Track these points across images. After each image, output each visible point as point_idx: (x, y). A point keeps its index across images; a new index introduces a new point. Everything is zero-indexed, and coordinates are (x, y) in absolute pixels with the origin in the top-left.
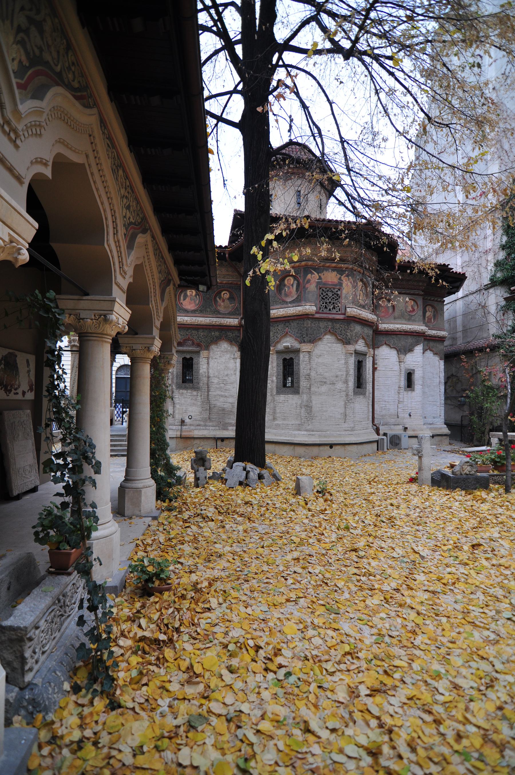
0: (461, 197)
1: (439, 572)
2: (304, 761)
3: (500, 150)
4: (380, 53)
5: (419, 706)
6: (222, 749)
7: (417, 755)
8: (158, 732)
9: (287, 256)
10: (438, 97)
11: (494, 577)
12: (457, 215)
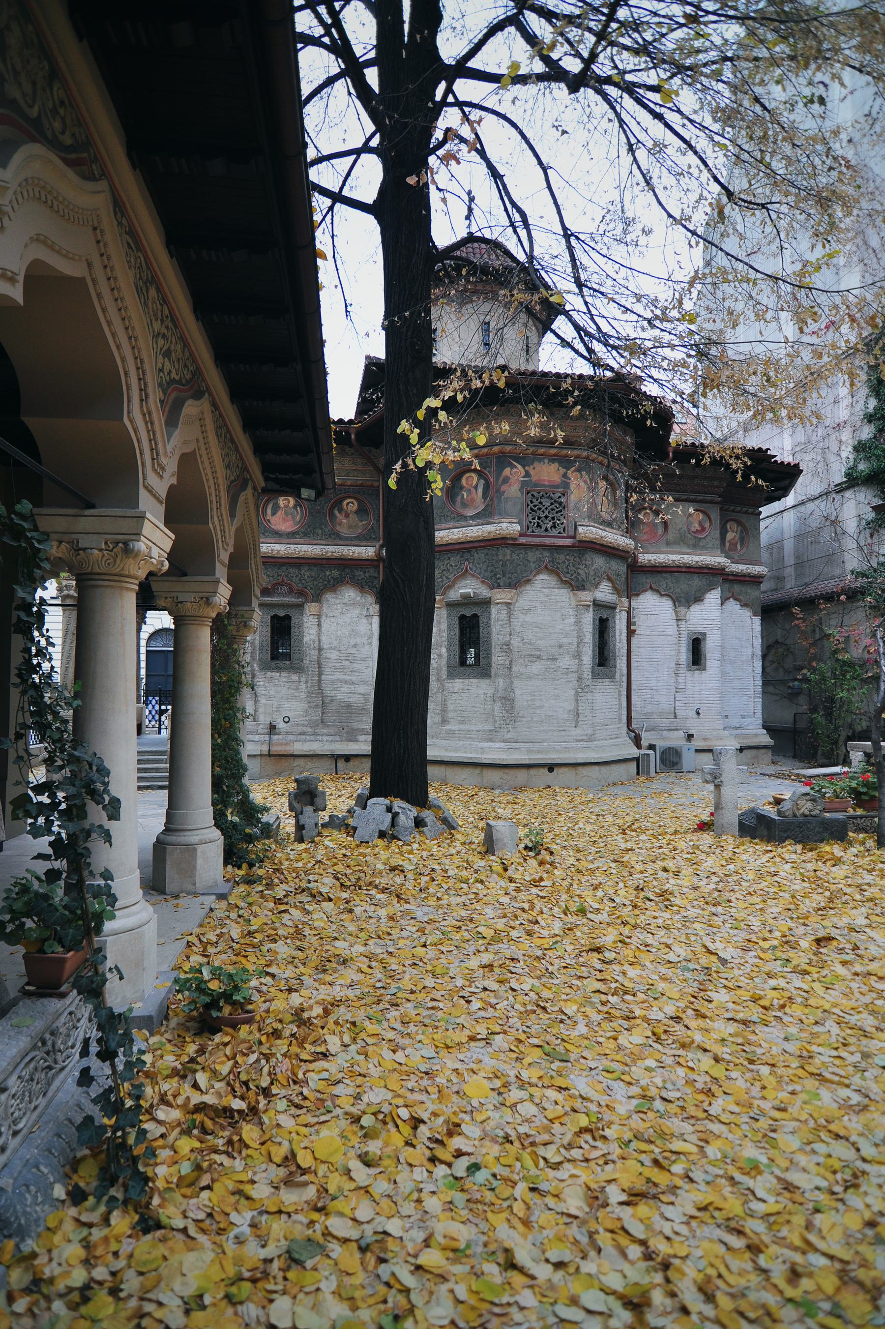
0: (790, 330)
1: (755, 987)
2: (504, 1319)
3: (863, 248)
4: (636, 80)
5: (720, 1221)
6: (351, 1299)
7: (717, 1307)
8: (231, 1271)
9: (465, 436)
10: (746, 156)
11: (858, 995)
12: (783, 362)
